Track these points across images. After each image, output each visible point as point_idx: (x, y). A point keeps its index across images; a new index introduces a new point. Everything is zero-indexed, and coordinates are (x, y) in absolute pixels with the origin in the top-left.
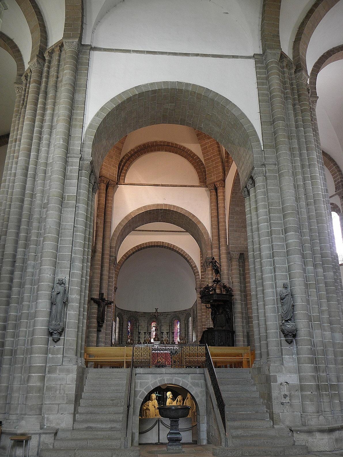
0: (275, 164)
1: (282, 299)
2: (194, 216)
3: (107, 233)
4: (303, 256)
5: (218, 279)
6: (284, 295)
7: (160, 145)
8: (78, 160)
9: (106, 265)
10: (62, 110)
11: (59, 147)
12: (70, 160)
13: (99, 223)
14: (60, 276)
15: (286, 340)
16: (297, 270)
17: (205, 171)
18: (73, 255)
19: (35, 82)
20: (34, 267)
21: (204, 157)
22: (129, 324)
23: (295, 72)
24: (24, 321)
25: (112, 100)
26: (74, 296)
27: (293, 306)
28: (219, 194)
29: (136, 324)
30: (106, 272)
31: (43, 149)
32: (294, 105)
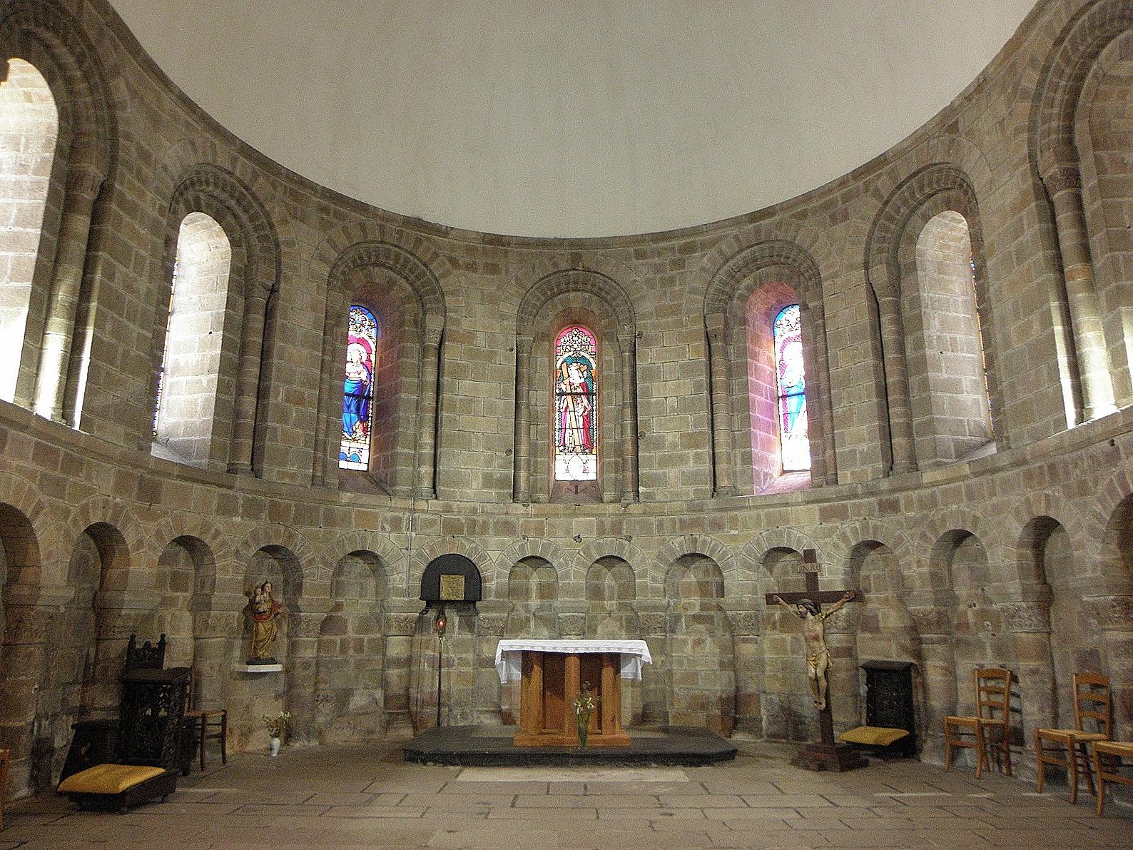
29: (419, 324)
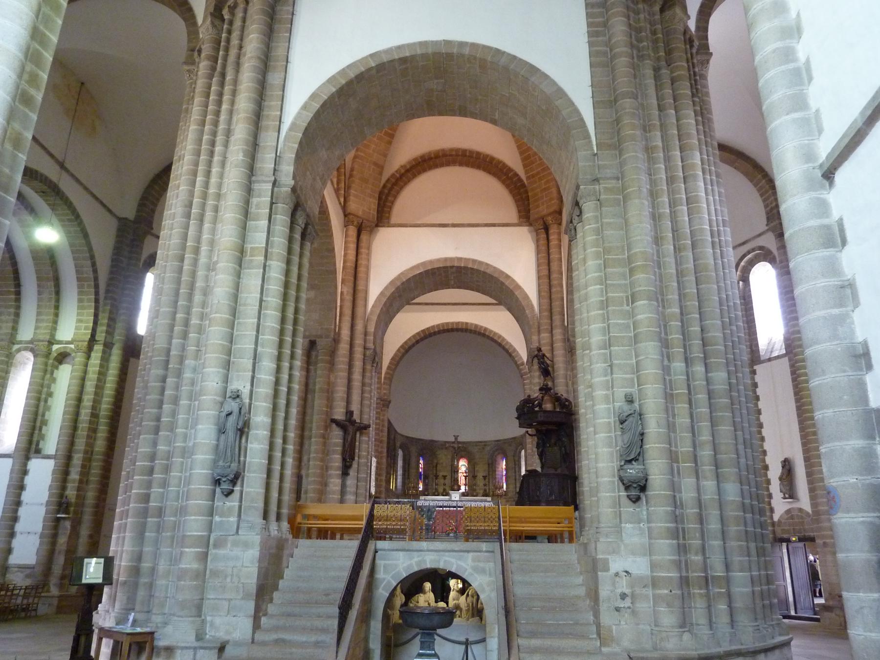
0: (618, 179)
1: (622, 422)
2: (508, 277)
3: (359, 311)
4: (665, 344)
5: (547, 385)
6: (626, 414)
7: (451, 155)
8: (269, 186)
9: (358, 364)
10: (244, 104)
11: (236, 166)
12: (256, 186)
13: (345, 293)
14: (234, 385)
15: (628, 496)
16: (651, 370)
17: (528, 198)
18: (259, 349)
19: (209, 58)
20: (194, 370)
21: (526, 172)
22: (421, 462)
23: (662, 10)
24: (177, 460)
25: (331, 80)
26: (260, 419)
27: (642, 434)
28: (551, 237)
30: (357, 376)
31: (215, 170)
32: (657, 70)
